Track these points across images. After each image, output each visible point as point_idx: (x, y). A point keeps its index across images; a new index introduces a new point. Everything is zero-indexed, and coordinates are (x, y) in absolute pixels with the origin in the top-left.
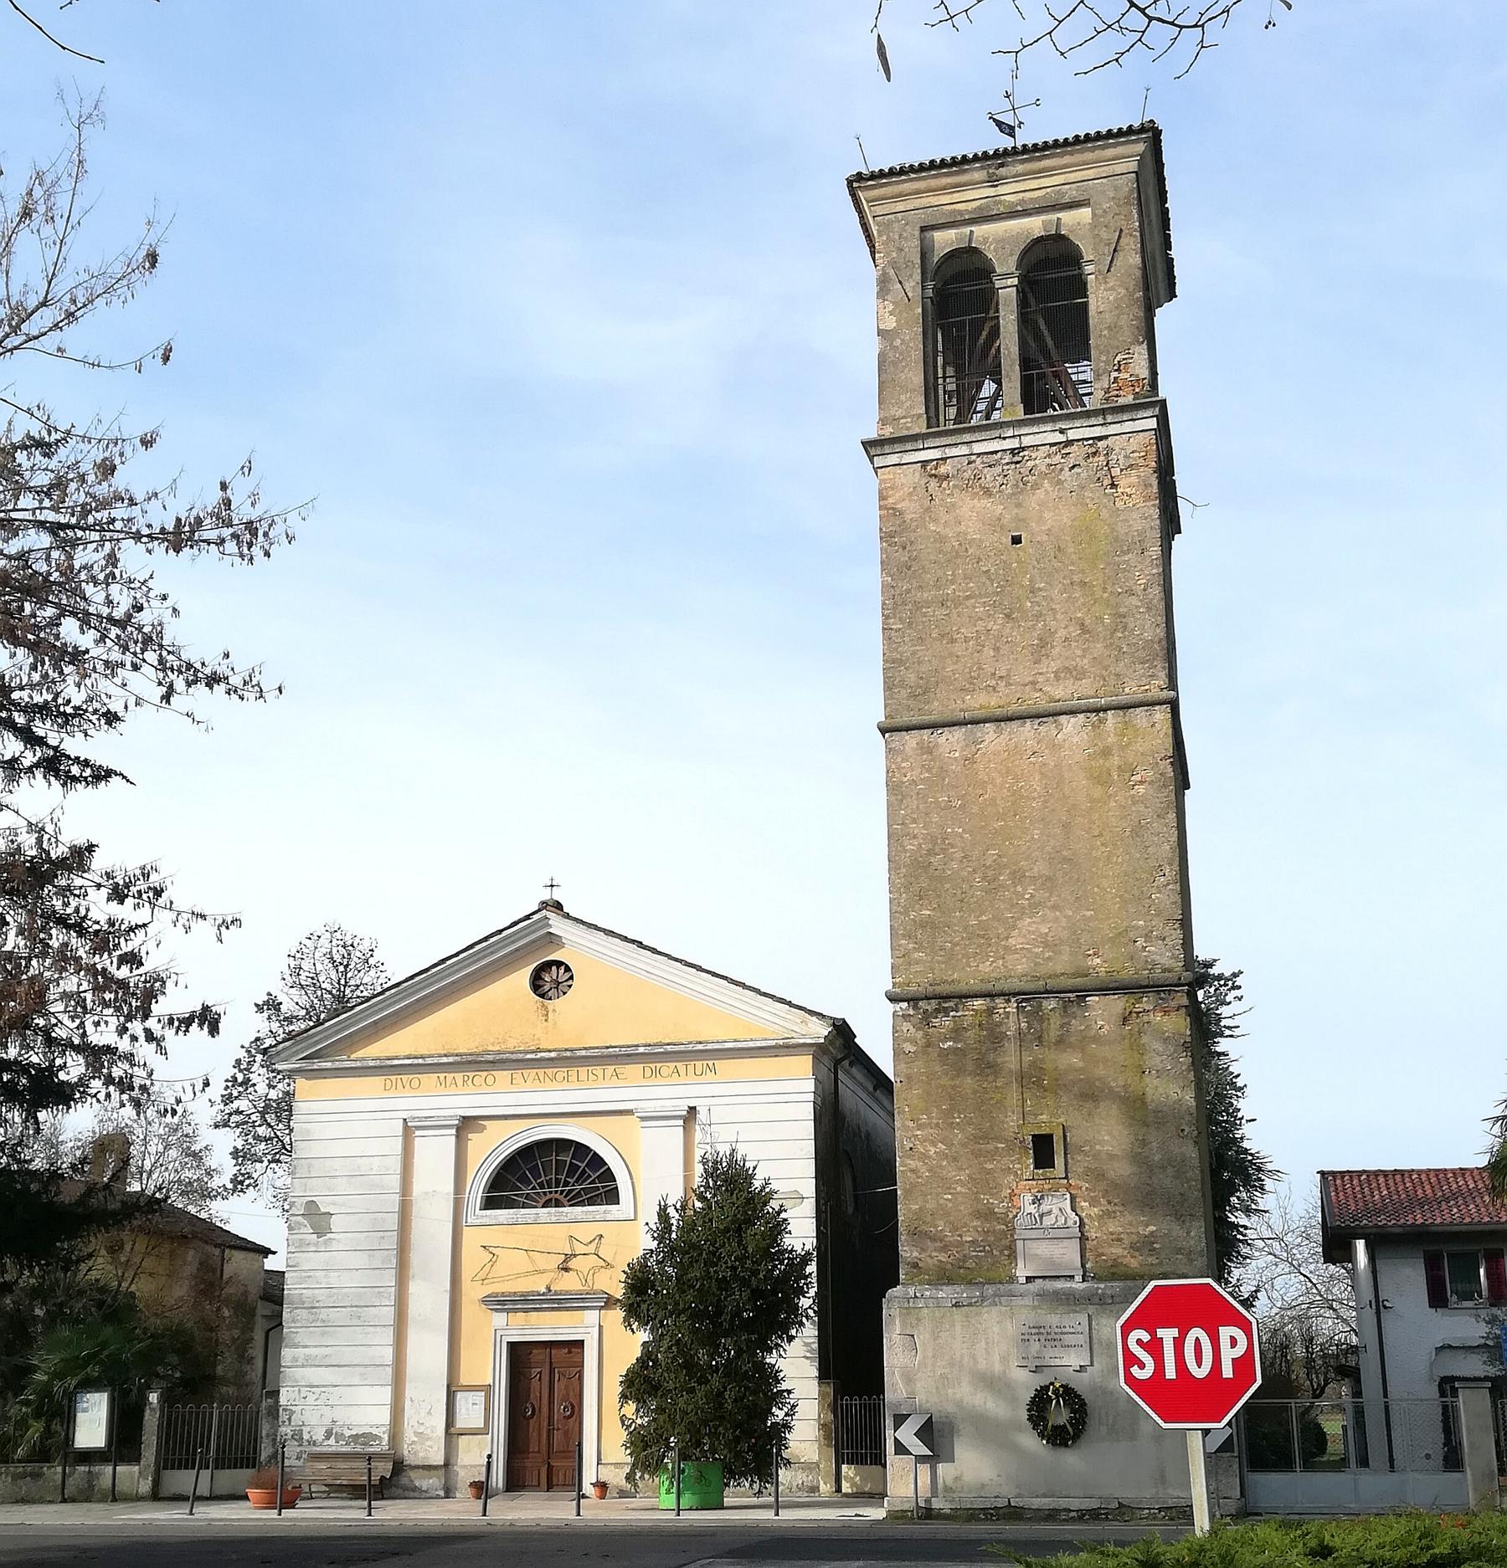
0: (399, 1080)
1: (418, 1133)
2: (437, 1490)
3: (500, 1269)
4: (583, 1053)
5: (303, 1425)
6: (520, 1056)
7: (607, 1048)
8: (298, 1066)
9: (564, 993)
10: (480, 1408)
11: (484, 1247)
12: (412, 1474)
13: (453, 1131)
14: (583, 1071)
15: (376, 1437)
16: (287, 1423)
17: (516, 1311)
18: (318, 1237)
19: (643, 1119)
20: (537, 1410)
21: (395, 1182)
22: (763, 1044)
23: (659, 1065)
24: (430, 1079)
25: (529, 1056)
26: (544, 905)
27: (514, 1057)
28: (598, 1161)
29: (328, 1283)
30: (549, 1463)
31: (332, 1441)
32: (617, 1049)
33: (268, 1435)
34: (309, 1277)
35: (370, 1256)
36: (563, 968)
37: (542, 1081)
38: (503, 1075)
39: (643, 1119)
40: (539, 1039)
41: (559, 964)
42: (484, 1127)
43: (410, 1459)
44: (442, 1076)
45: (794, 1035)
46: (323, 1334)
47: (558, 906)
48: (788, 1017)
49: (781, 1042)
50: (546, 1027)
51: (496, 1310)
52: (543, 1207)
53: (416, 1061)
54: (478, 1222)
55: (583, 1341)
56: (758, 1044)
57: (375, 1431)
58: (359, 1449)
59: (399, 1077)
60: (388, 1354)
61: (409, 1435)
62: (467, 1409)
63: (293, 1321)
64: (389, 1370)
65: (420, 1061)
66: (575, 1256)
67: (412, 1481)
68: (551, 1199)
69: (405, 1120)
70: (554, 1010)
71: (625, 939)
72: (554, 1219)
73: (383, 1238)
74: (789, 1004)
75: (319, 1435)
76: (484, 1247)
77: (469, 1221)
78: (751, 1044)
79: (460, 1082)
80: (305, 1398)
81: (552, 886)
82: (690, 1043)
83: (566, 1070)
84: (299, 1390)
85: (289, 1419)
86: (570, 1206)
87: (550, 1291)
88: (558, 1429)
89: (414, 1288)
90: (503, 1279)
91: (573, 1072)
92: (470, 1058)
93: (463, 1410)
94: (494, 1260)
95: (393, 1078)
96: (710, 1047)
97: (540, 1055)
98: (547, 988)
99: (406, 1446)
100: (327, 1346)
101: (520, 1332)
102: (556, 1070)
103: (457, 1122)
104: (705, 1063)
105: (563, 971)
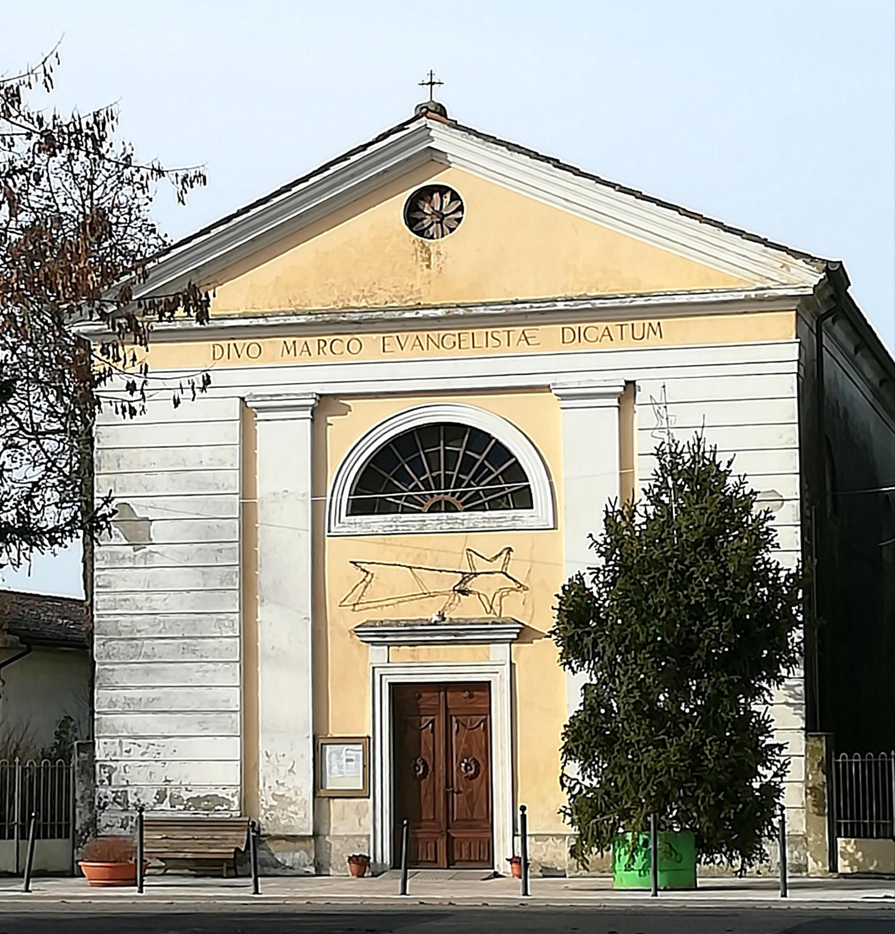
0: (232, 346)
1: (260, 416)
2: (305, 866)
3: (376, 591)
4: (481, 310)
5: (128, 785)
6: (397, 315)
7: (514, 303)
8: (97, 328)
9: (451, 230)
10: (357, 767)
11: (354, 563)
12: (272, 846)
13: (308, 414)
14: (480, 333)
15: (223, 801)
16: (107, 782)
17: (399, 644)
18: (135, 550)
19: (563, 397)
20: (430, 768)
21: (233, 480)
22: (729, 297)
23: (583, 326)
24: (273, 346)
25: (408, 315)
26: (423, 111)
27: (387, 315)
28: (501, 453)
29: (150, 608)
30: (448, 834)
31: (166, 805)
32: (528, 305)
33: (82, 798)
34: (125, 600)
35: (203, 573)
36: (448, 195)
37: (425, 347)
38: (371, 341)
39: (563, 397)
40: (419, 291)
41: (443, 190)
42: (349, 408)
43: (268, 829)
44: (289, 341)
45: (771, 284)
46: (147, 672)
47: (441, 111)
48: (764, 260)
49: (753, 295)
50: (429, 276)
51: (373, 643)
52: (429, 512)
53: (255, 322)
54: (345, 530)
55: (489, 682)
56: (721, 297)
57: (221, 793)
58: (201, 815)
59: (232, 342)
60: (234, 697)
61: (265, 798)
62: (340, 767)
63: (108, 656)
64: (237, 717)
65: (261, 321)
66: (476, 574)
67: (272, 855)
68: (439, 502)
69: (242, 399)
70: (439, 253)
71: (536, 156)
72: (446, 527)
73: (220, 551)
74: (765, 242)
75: (149, 799)
76: (354, 563)
77: (333, 529)
78: (712, 298)
79: (314, 349)
80: (128, 752)
81: (432, 83)
82: (628, 296)
83: (456, 332)
84: (120, 742)
85: (109, 778)
86: (466, 510)
87: (444, 619)
88: (459, 792)
89: (264, 614)
90: (381, 604)
91: (466, 335)
92: (327, 317)
93: (335, 769)
94: (368, 579)
95: (224, 343)
96: (654, 301)
97: (421, 313)
98: (426, 222)
99: (263, 812)
100: (154, 687)
101: (405, 671)
102: (443, 333)
103: (312, 402)
104: (647, 322)
105: (447, 200)
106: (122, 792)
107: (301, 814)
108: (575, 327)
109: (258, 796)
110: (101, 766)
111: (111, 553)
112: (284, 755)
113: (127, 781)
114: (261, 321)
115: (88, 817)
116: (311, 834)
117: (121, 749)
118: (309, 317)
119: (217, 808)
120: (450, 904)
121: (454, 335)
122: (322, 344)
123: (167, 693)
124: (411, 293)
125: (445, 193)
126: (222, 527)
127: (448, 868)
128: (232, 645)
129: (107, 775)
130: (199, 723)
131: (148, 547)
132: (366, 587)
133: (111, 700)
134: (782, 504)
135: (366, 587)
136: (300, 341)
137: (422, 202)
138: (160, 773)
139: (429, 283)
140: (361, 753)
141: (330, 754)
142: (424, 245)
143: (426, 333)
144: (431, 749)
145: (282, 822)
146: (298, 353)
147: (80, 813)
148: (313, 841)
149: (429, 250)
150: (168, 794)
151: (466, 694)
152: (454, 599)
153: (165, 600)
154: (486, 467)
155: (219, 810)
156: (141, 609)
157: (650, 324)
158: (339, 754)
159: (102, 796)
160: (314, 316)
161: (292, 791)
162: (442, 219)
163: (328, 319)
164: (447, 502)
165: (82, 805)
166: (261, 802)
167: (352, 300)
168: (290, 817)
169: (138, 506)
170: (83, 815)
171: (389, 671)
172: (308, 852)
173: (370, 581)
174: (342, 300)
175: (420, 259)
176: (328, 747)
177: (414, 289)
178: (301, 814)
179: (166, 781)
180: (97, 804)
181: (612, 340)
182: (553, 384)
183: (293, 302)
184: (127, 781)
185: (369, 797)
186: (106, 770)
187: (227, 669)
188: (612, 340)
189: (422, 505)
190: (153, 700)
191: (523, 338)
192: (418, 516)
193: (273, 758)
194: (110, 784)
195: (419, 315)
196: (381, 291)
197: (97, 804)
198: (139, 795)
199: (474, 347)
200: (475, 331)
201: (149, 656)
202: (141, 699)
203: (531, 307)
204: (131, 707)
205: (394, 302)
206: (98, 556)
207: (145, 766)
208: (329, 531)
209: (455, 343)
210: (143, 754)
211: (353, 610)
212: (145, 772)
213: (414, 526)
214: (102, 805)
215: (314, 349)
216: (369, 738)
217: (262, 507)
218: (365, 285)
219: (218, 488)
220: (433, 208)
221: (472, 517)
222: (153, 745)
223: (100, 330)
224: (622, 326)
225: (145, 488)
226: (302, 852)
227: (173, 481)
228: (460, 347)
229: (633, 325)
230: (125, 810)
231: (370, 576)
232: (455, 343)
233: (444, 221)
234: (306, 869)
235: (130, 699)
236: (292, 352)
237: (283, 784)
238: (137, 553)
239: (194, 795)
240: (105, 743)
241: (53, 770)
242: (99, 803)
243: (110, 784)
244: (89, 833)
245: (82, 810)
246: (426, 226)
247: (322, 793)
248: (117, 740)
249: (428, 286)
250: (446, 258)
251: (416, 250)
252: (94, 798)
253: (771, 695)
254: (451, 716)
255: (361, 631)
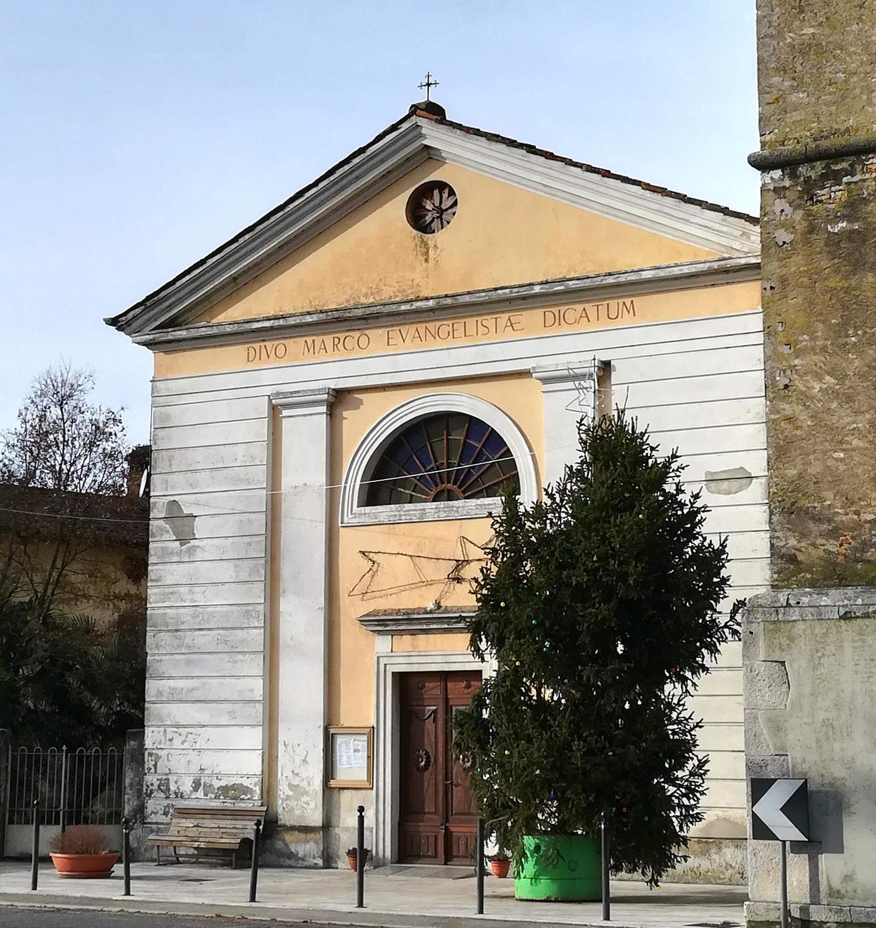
0: (263, 347)
1: (285, 413)
2: (314, 858)
3: (383, 581)
4: (467, 299)
5: (170, 773)
6: (393, 308)
7: (496, 289)
8: (151, 337)
9: (448, 223)
10: (362, 758)
11: (363, 553)
12: (288, 837)
13: (324, 409)
14: (471, 322)
15: (246, 790)
16: (153, 770)
17: (401, 633)
18: (182, 545)
19: (545, 380)
20: (432, 760)
21: (261, 474)
22: (693, 269)
23: (563, 309)
24: (296, 345)
25: (403, 307)
27: (386, 309)
28: (495, 441)
29: (192, 600)
30: (447, 828)
31: (200, 794)
32: (508, 290)
33: (131, 785)
34: (172, 593)
35: (236, 566)
36: (447, 191)
37: (423, 340)
38: (377, 335)
39: (545, 380)
40: (418, 285)
41: (442, 186)
42: (361, 402)
43: (285, 819)
44: (310, 340)
46: (188, 663)
49: (715, 265)
50: (427, 269)
51: (379, 632)
52: (434, 501)
53: (276, 323)
54: (355, 521)
55: (481, 671)
56: (686, 270)
57: (246, 782)
58: (229, 805)
59: (263, 344)
60: (257, 687)
61: (283, 790)
62: (349, 757)
63: (157, 647)
64: (260, 707)
65: (281, 322)
66: (468, 562)
67: (286, 845)
68: (443, 490)
69: (269, 396)
70: (435, 246)
72: (443, 515)
73: (249, 544)
75: (187, 786)
76: (363, 553)
77: (346, 520)
78: (676, 271)
79: (329, 347)
80: (171, 740)
82: (598, 276)
83: (450, 322)
84: (165, 731)
85: (155, 766)
86: (466, 498)
87: (439, 607)
88: (457, 785)
89: (285, 605)
90: (384, 594)
91: (459, 325)
92: (336, 314)
93: (344, 758)
94: (374, 569)
95: (257, 346)
96: (622, 279)
97: (417, 305)
98: (428, 218)
99: (280, 802)
100: (193, 677)
101: (406, 660)
102: (438, 324)
103: (326, 396)
104: (621, 301)
105: (445, 195)
106: (165, 779)
107: (312, 805)
108: (555, 310)
109: (277, 787)
110: (149, 754)
111: (163, 548)
112: (299, 745)
113: (169, 769)
114: (281, 322)
115: (135, 804)
116: (319, 823)
117: (165, 737)
118: (321, 315)
119: (242, 797)
120: (244, 918)
121: (448, 326)
122: (336, 340)
123: (204, 684)
124: (412, 287)
125: (445, 188)
126: (252, 521)
127: (445, 864)
128: (257, 635)
129: (154, 763)
130: (229, 712)
131: (191, 541)
132: (373, 576)
133: (158, 690)
134: (751, 482)
135: (373, 576)
136: (318, 339)
137: (424, 200)
138: (197, 761)
139: (427, 276)
140: (366, 743)
141: (340, 744)
142: (423, 240)
143: (424, 325)
144: (433, 740)
145: (297, 812)
146: (316, 352)
147: (129, 800)
148: (321, 832)
149: (427, 245)
150: (202, 782)
151: (464, 684)
152: (449, 587)
153: (204, 592)
154: (485, 454)
155: (243, 799)
156: (185, 601)
157: (624, 303)
158: (348, 745)
159: (149, 784)
160: (325, 314)
161: (305, 782)
162: (441, 215)
163: (336, 316)
164: (449, 491)
165: (130, 792)
166: (280, 792)
167: (362, 298)
168: (303, 807)
169: (185, 503)
170: (131, 802)
171: (393, 660)
172: (316, 843)
173: (377, 571)
174: (354, 298)
175: (419, 254)
176: (338, 736)
177: (415, 283)
178: (312, 805)
179: (201, 769)
180: (145, 791)
181: (589, 321)
182: (534, 368)
183: (313, 303)
184: (169, 769)
185: (372, 789)
186: (153, 758)
187: (252, 659)
188: (589, 321)
189: (428, 495)
190: (192, 689)
191: (509, 324)
192: (420, 506)
193: (290, 747)
194: (156, 772)
195: (413, 307)
196: (387, 287)
197: (145, 791)
198: (179, 783)
199: (465, 336)
200: (466, 320)
201: (189, 647)
202: (182, 689)
203: (511, 292)
204: (176, 698)
205: (397, 296)
206: (152, 551)
207: (184, 754)
208: (342, 523)
209: (449, 332)
210: (183, 743)
211: (363, 600)
212: (184, 760)
213: (415, 515)
214: (149, 792)
215: (329, 347)
216: (373, 727)
217: (285, 501)
218: (373, 283)
219: (249, 484)
220: (433, 204)
221: (467, 504)
222: (192, 733)
223: (154, 339)
224: (598, 306)
225: (191, 485)
226: (312, 843)
227: (213, 478)
228: (453, 337)
229: (608, 304)
230: (167, 797)
231: (376, 565)
232: (449, 332)
233: (444, 216)
234: (315, 861)
235: (173, 689)
236: (311, 350)
237: (297, 774)
238: (183, 547)
239: (223, 783)
240: (153, 732)
241: (104, 757)
242: (147, 790)
243: (156, 772)
244: (136, 820)
245: (130, 797)
246: (428, 222)
247: (333, 783)
248: (162, 729)
249: (426, 279)
250: (442, 250)
251: (416, 245)
252: (142, 786)
253: (694, 685)
254: (451, 706)
255: (365, 621)
